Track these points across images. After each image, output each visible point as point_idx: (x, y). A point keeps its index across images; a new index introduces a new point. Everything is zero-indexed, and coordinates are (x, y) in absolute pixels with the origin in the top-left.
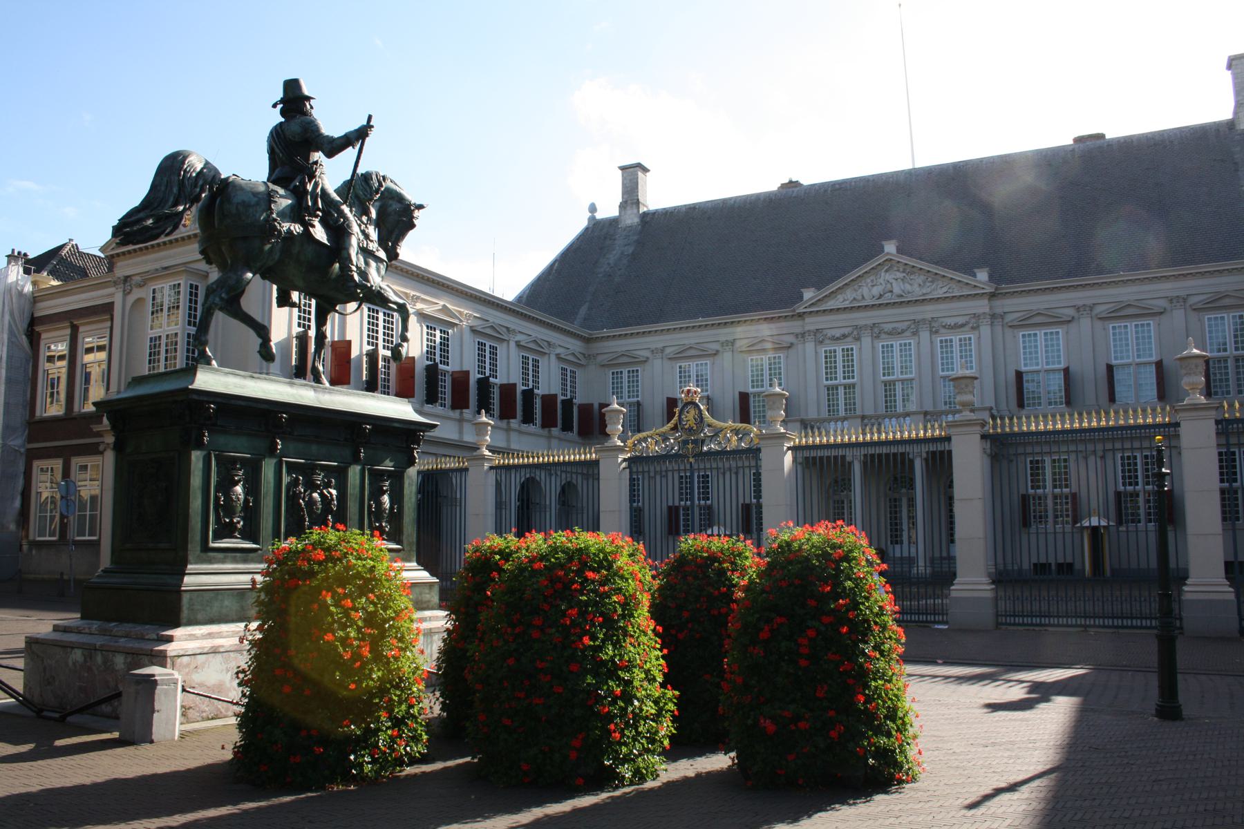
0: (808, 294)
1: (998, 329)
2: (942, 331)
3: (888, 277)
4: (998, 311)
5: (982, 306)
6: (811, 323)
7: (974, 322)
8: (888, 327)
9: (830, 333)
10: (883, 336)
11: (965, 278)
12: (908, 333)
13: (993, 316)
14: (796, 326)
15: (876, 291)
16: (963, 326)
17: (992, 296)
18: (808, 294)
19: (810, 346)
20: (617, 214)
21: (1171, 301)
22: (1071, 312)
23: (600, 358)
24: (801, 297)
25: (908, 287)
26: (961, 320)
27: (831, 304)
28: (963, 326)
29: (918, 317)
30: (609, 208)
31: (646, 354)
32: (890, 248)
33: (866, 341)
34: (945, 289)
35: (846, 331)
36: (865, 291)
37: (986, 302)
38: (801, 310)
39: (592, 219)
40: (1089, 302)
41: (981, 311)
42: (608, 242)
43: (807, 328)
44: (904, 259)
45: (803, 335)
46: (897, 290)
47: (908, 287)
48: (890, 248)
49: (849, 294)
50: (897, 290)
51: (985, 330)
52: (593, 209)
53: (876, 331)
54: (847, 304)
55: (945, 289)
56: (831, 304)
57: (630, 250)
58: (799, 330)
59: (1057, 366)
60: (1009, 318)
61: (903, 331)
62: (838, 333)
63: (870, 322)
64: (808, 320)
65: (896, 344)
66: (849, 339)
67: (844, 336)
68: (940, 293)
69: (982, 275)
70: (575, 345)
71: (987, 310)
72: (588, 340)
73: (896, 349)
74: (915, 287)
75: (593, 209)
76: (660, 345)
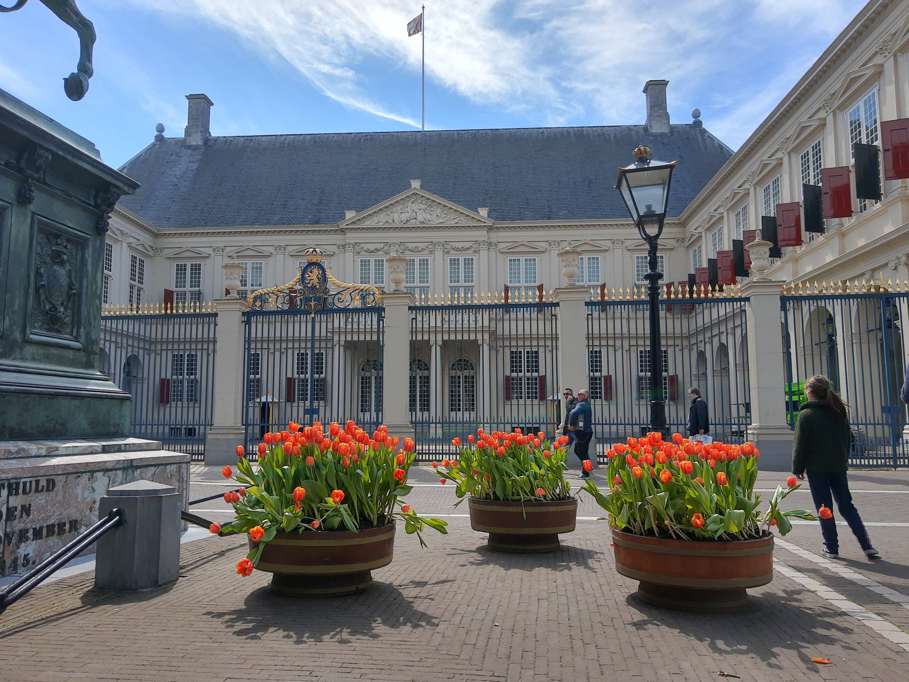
0: (350, 215)
1: (493, 254)
2: (452, 252)
3: (415, 207)
4: (494, 240)
5: (482, 235)
6: (351, 237)
8: (411, 246)
9: (366, 247)
12: (426, 252)
13: (490, 244)
14: (337, 239)
15: (404, 217)
16: (467, 249)
17: (490, 229)
18: (350, 215)
19: (349, 255)
20: (181, 134)
22: (545, 245)
23: (166, 251)
24: (343, 217)
25: (427, 216)
27: (367, 224)
28: (467, 249)
29: (435, 240)
30: (177, 126)
31: (209, 251)
32: (416, 184)
34: (456, 221)
35: (379, 246)
37: (484, 233)
38: (343, 226)
39: (160, 139)
40: (557, 239)
42: (173, 157)
43: (347, 241)
44: (427, 195)
45: (344, 246)
46: (420, 218)
47: (427, 216)
48: (416, 184)
50: (420, 218)
51: (484, 253)
52: (160, 129)
54: (380, 225)
55: (456, 221)
56: (367, 224)
57: (195, 166)
58: (340, 243)
59: (533, 284)
61: (423, 250)
62: (372, 247)
63: (398, 241)
68: (452, 223)
69: (483, 212)
70: (146, 238)
71: (486, 239)
72: (156, 235)
74: (435, 216)
75: (160, 129)
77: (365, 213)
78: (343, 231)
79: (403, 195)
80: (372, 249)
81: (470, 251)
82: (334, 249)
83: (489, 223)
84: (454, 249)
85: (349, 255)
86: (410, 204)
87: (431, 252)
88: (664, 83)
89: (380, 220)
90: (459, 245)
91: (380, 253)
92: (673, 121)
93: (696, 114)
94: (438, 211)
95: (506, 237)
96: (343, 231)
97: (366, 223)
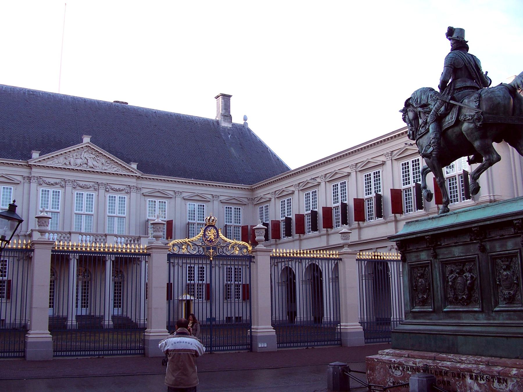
0: (35, 155)
2: (111, 191)
3: (86, 155)
4: (139, 186)
5: (132, 182)
6: (36, 172)
7: (128, 190)
8: (81, 183)
9: (47, 180)
10: (78, 188)
11: (124, 164)
12: (92, 189)
14: (25, 172)
15: (79, 161)
17: (138, 178)
18: (35, 155)
21: (213, 197)
22: (172, 193)
25: (95, 163)
26: (122, 187)
27: (49, 163)
28: (122, 190)
29: (100, 181)
32: (87, 139)
33: (69, 188)
34: (115, 169)
35: (58, 181)
36: (72, 161)
37: (134, 180)
40: (181, 190)
41: (131, 185)
43: (33, 175)
46: (90, 164)
48: (87, 139)
49: (61, 159)
50: (90, 164)
53: (76, 185)
55: (115, 169)
58: (26, 175)
60: (144, 191)
62: (52, 181)
63: (72, 179)
64: (34, 170)
65: (85, 193)
66: (58, 186)
67: (56, 184)
69: (134, 166)
71: (135, 185)
73: (85, 196)
77: (50, 155)
78: (30, 167)
79: (79, 146)
80: (52, 183)
81: (123, 192)
82: (20, 179)
84: (112, 189)
85: (34, 185)
86: (83, 153)
87: (95, 190)
88: (230, 96)
89: (59, 162)
90: (117, 187)
91: (57, 186)
92: (234, 121)
93: (245, 119)
94: (103, 160)
97: (48, 163)
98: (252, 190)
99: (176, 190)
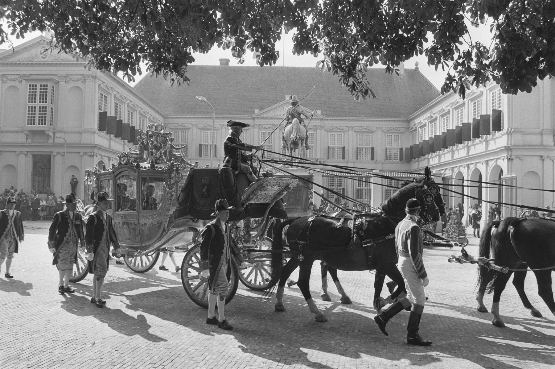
0: (257, 111)
1: (323, 131)
4: (323, 125)
9: (264, 126)
13: (321, 127)
18: (257, 111)
27: (265, 116)
43: (256, 123)
49: (272, 112)
54: (271, 116)
56: (265, 116)
62: (267, 126)
64: (256, 120)
71: (320, 124)
76: (196, 123)
78: (253, 119)
83: (321, 118)
89: (271, 114)
95: (329, 124)
96: (253, 119)
98: (409, 122)
99: (349, 125)
